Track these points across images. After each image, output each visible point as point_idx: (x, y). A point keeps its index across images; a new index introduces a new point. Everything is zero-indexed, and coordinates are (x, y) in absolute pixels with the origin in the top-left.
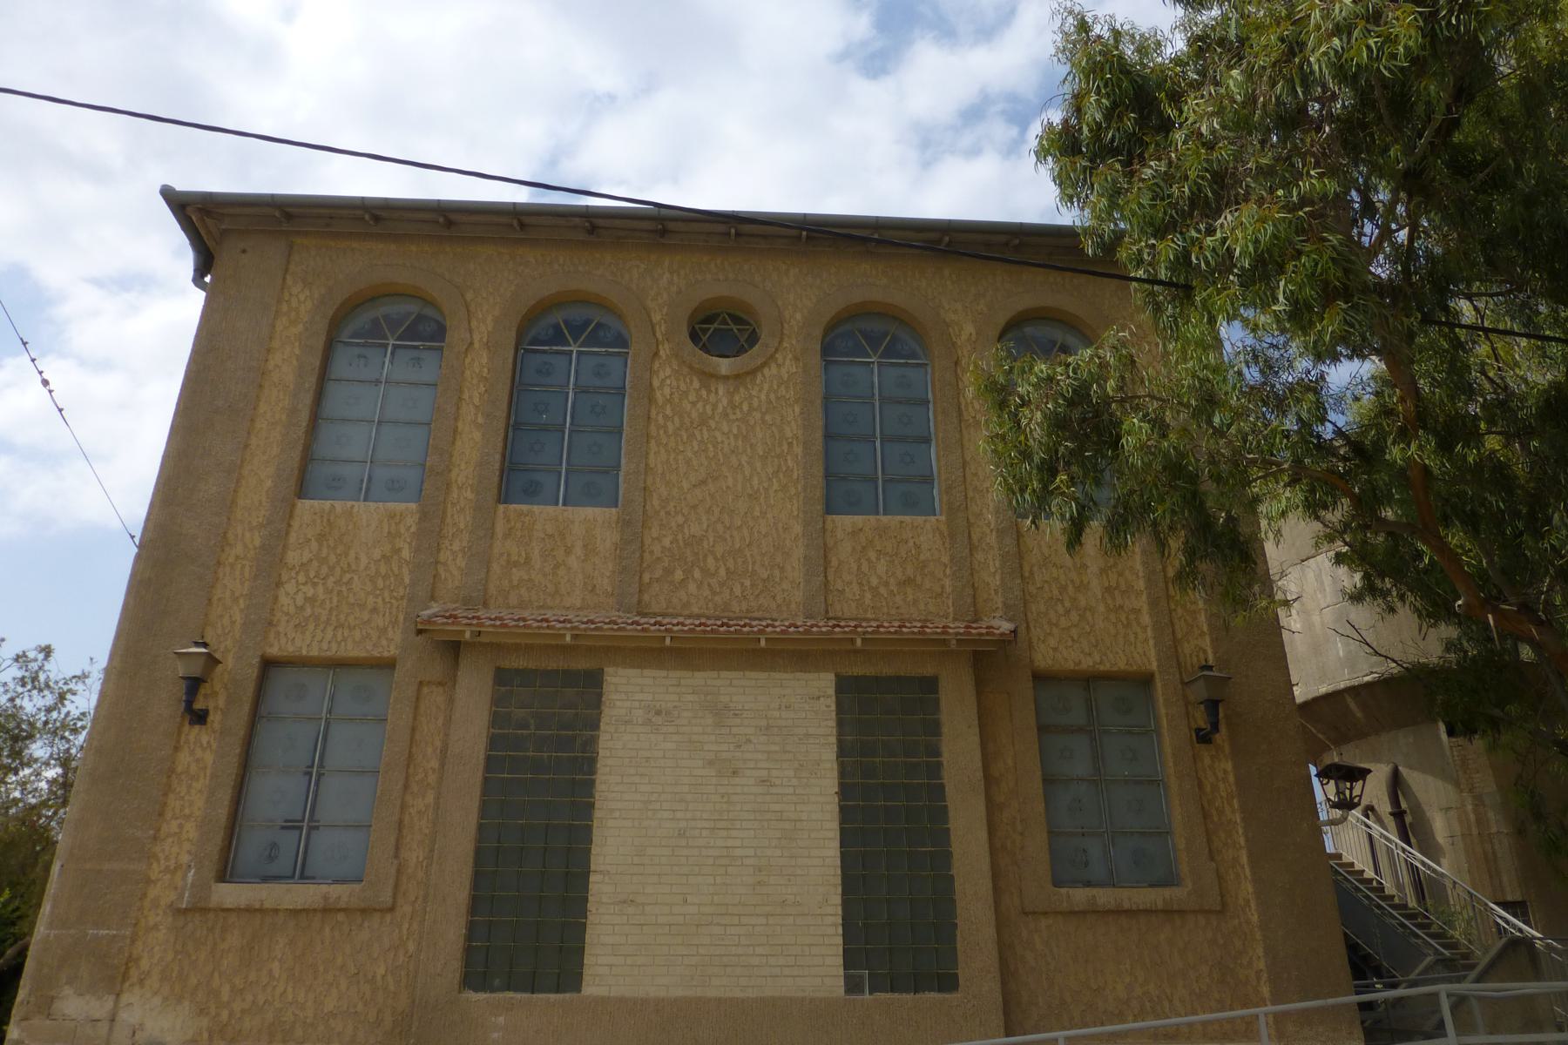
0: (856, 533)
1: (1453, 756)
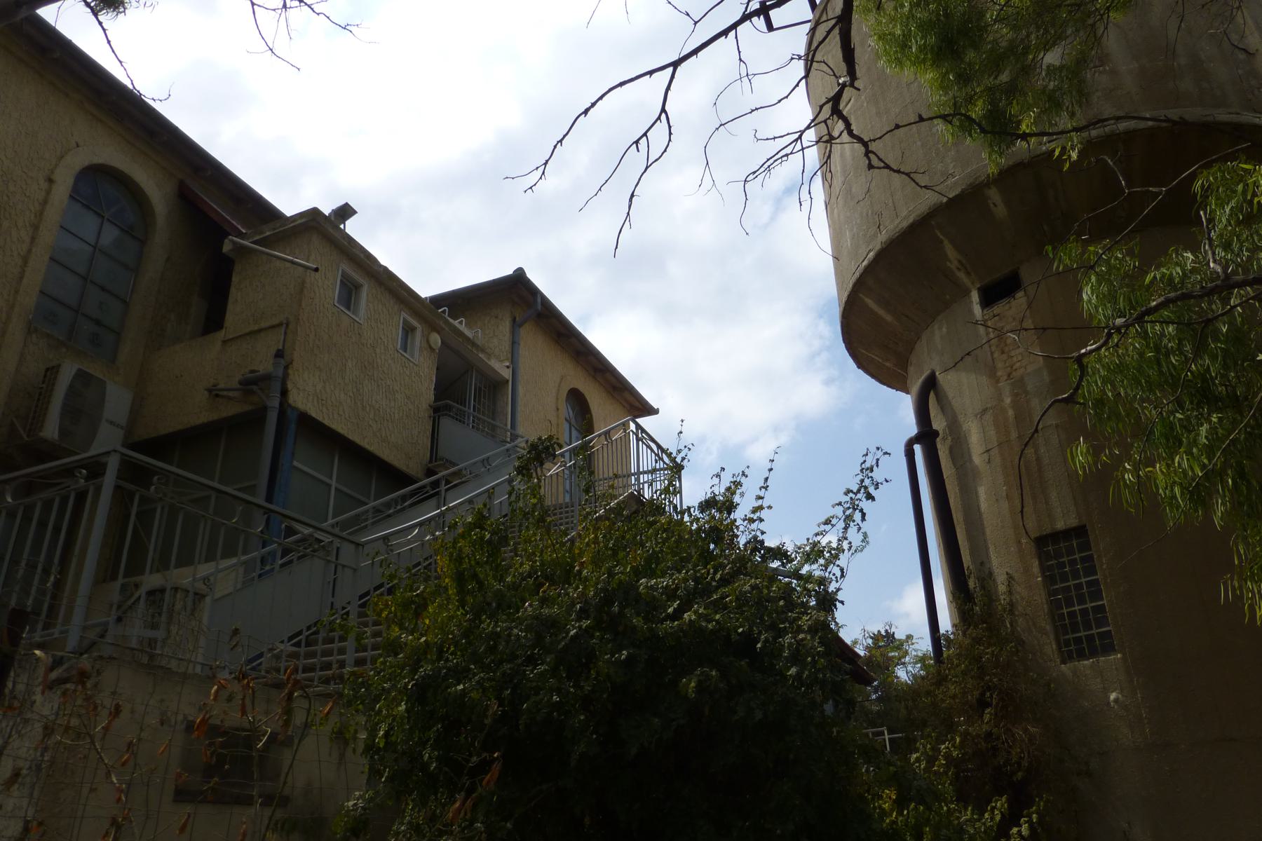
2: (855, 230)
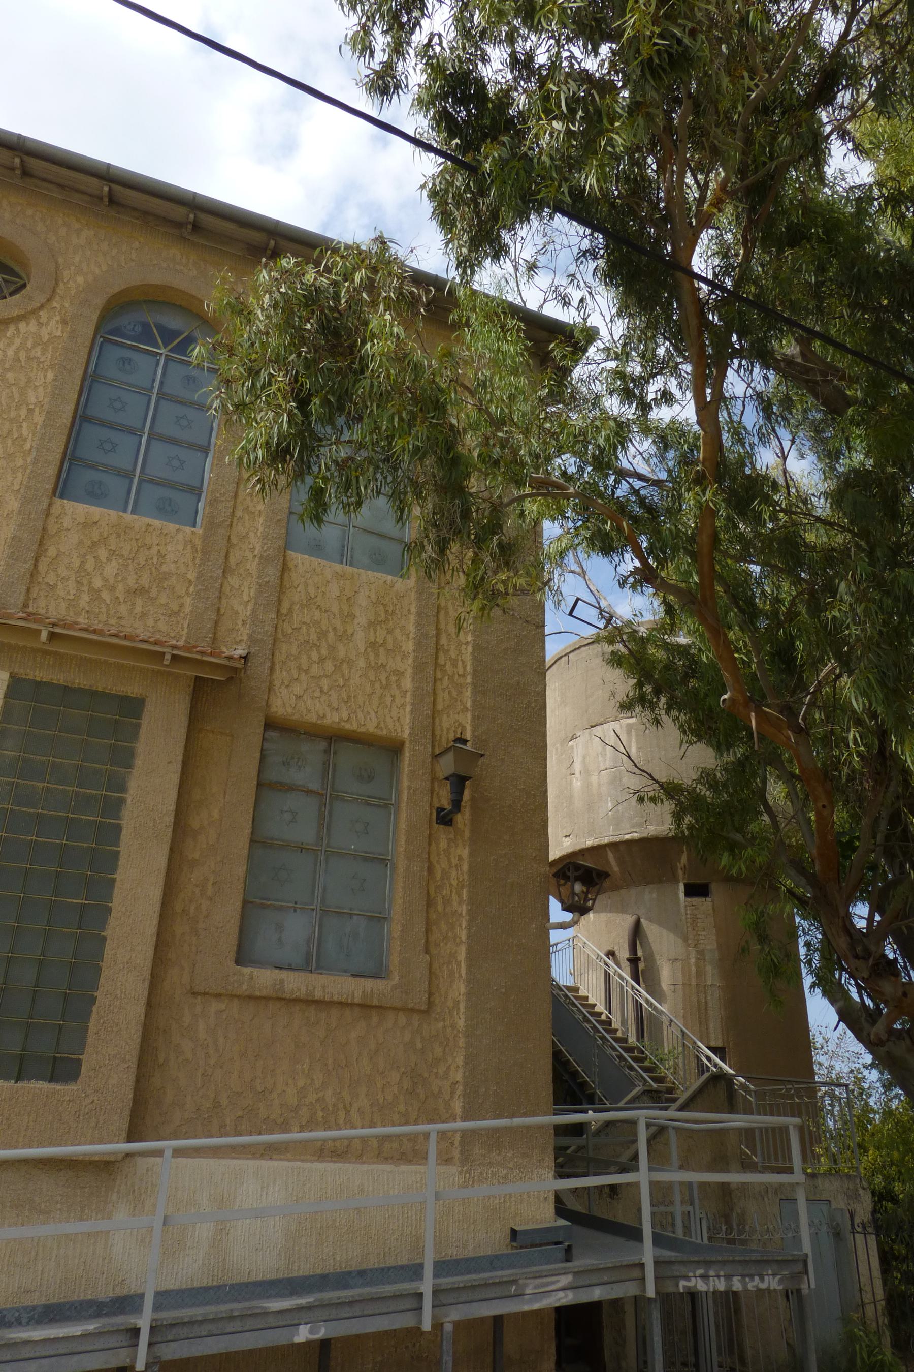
0: (88, 525)
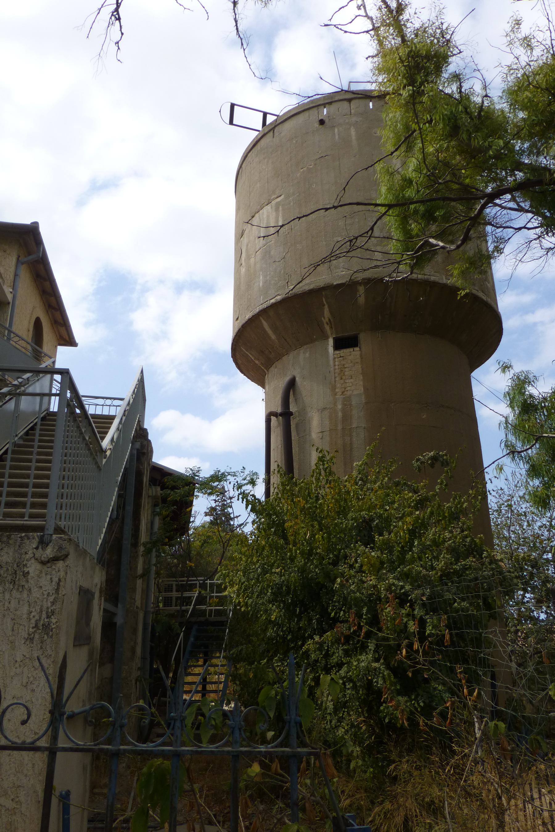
1: (335, 366)
2: (268, 278)
